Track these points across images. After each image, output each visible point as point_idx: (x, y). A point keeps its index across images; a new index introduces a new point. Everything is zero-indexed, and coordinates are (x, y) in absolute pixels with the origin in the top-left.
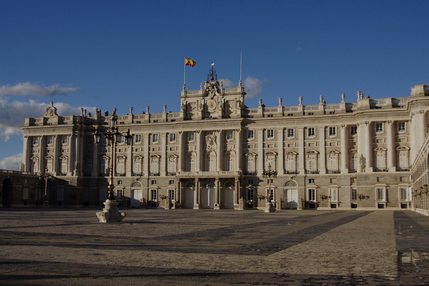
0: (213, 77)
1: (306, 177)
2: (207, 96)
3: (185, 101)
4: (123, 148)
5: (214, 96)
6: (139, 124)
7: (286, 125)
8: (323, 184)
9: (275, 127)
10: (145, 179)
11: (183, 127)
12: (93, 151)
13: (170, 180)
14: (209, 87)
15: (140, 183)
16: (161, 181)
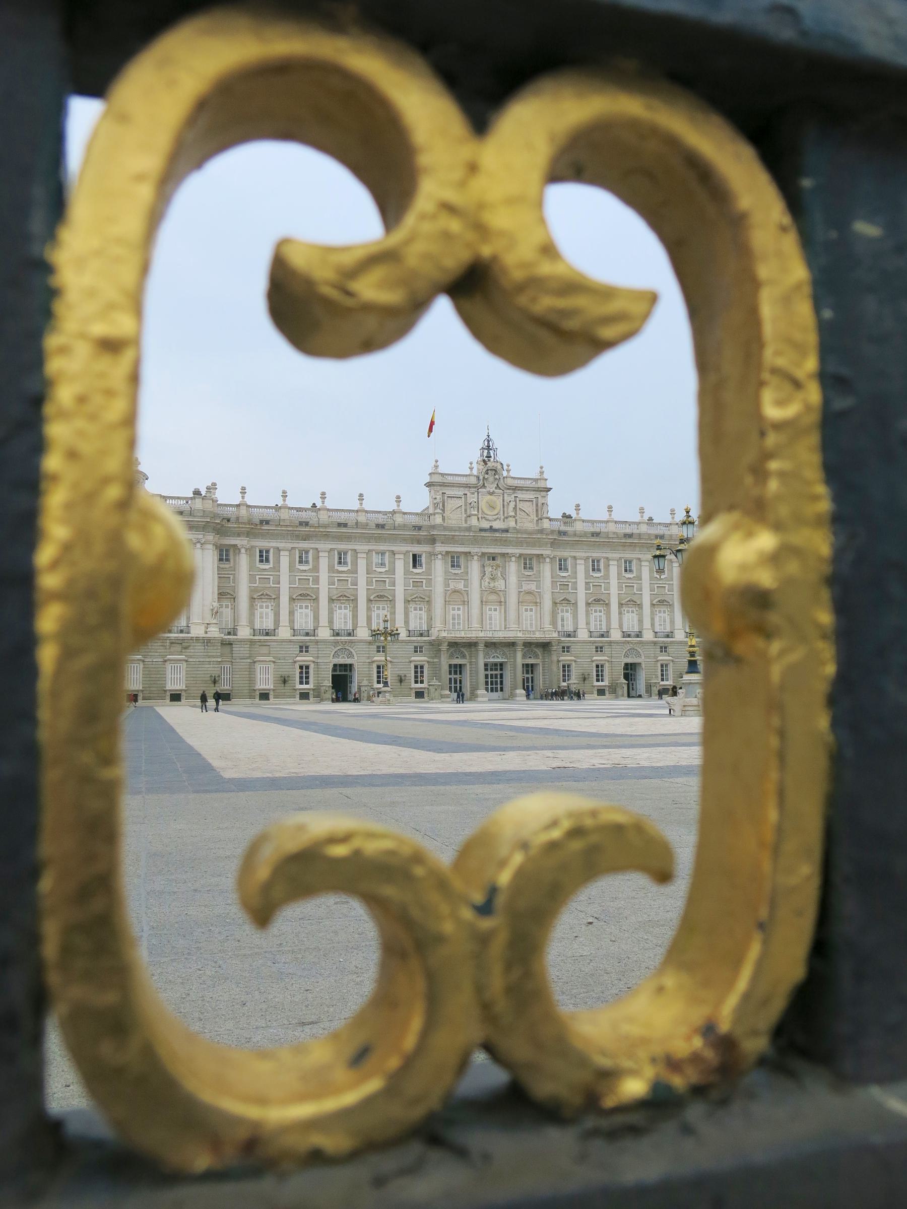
0: (489, 453)
1: (655, 643)
2: (484, 486)
3: (441, 492)
4: (306, 576)
5: (496, 488)
6: (344, 530)
7: (624, 553)
8: (681, 655)
9: (605, 555)
10: (362, 644)
11: (442, 543)
12: (234, 579)
13: (416, 644)
14: (488, 470)
15: (352, 650)
16: (397, 647)
